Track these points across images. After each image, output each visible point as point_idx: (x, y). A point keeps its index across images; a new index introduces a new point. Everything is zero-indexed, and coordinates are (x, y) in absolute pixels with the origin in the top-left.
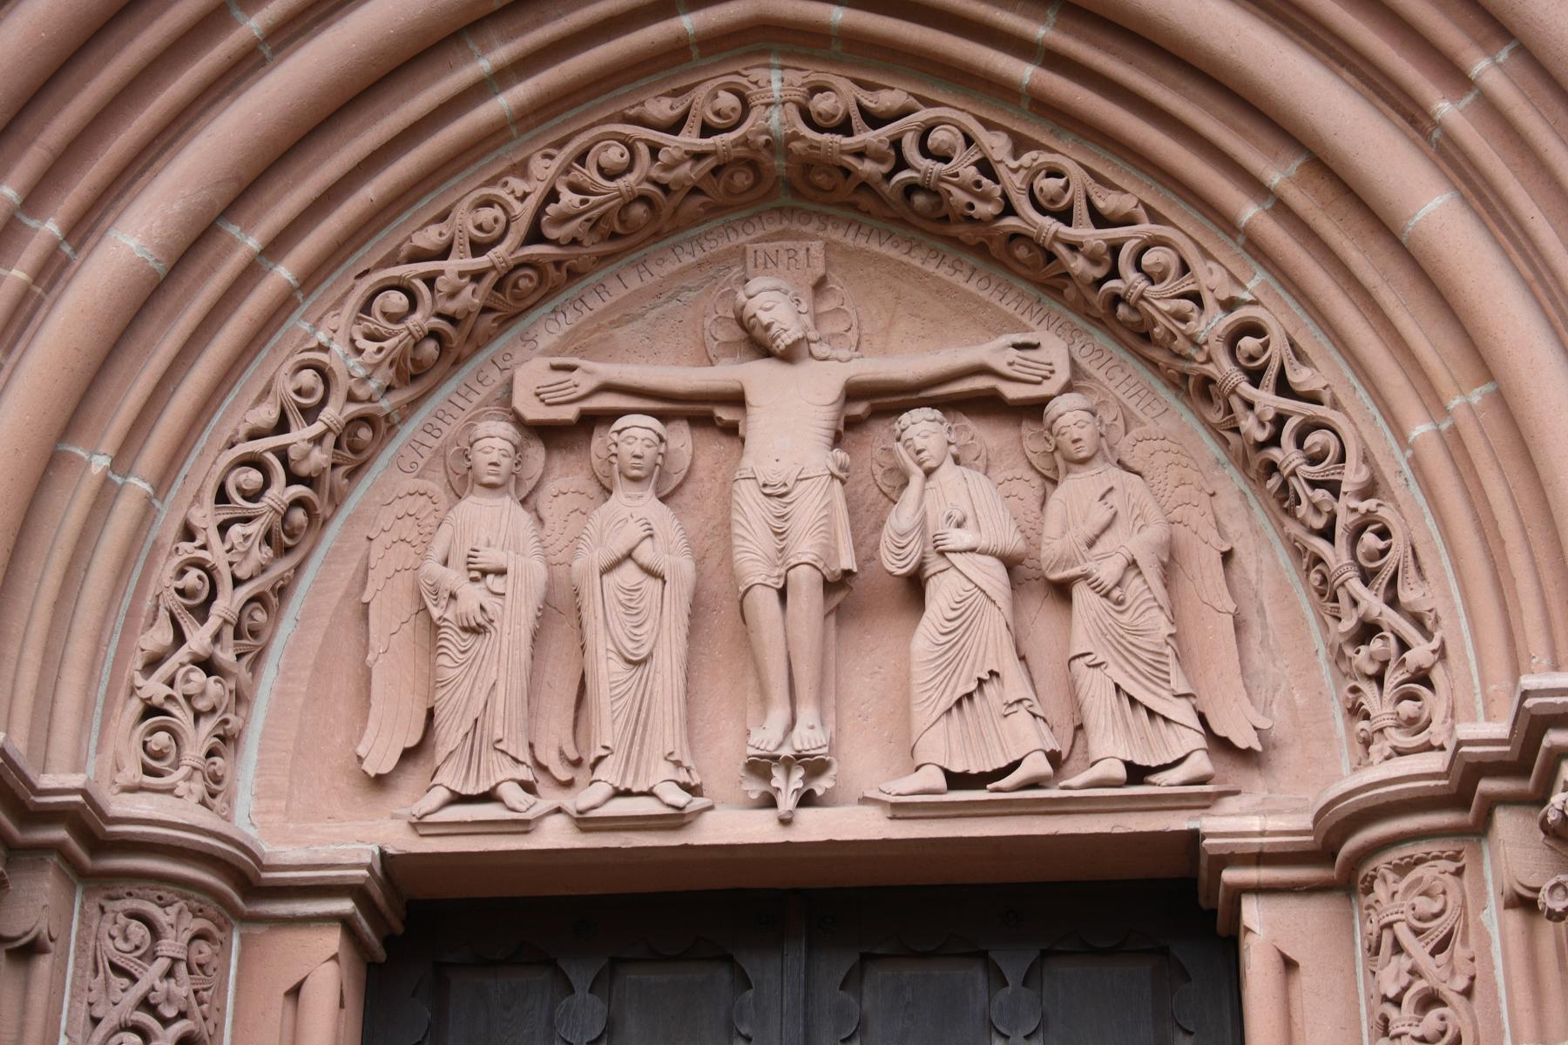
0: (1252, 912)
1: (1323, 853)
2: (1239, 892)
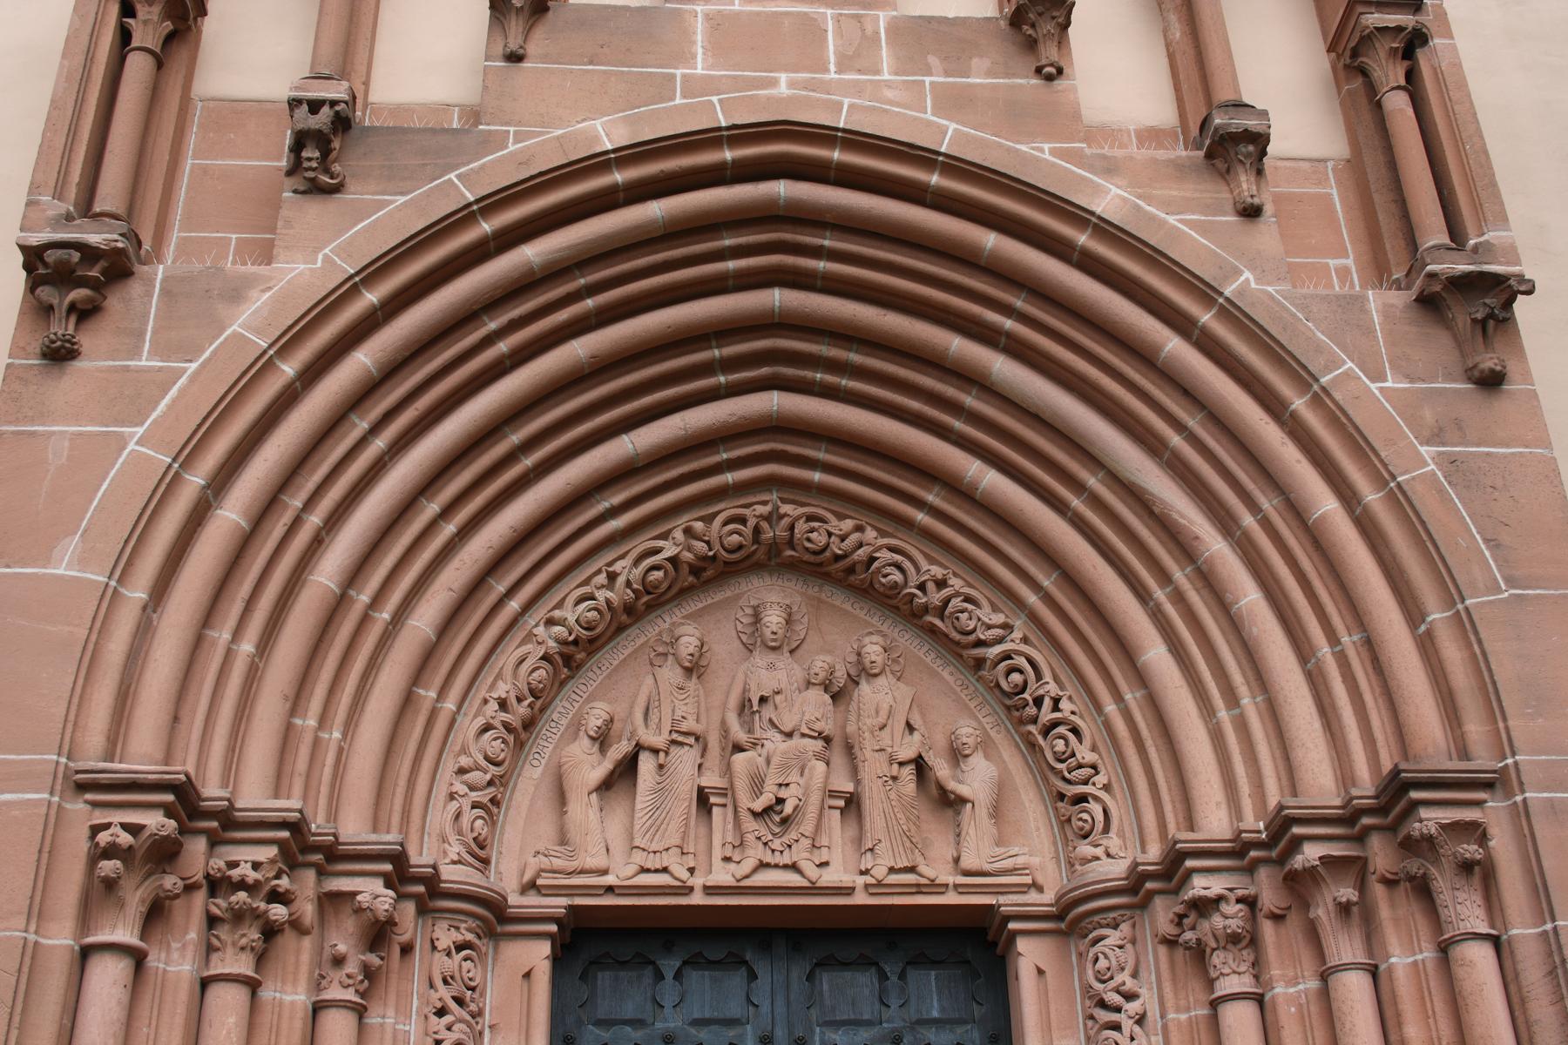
0: (1022, 944)
1: (1059, 917)
2: (1014, 934)
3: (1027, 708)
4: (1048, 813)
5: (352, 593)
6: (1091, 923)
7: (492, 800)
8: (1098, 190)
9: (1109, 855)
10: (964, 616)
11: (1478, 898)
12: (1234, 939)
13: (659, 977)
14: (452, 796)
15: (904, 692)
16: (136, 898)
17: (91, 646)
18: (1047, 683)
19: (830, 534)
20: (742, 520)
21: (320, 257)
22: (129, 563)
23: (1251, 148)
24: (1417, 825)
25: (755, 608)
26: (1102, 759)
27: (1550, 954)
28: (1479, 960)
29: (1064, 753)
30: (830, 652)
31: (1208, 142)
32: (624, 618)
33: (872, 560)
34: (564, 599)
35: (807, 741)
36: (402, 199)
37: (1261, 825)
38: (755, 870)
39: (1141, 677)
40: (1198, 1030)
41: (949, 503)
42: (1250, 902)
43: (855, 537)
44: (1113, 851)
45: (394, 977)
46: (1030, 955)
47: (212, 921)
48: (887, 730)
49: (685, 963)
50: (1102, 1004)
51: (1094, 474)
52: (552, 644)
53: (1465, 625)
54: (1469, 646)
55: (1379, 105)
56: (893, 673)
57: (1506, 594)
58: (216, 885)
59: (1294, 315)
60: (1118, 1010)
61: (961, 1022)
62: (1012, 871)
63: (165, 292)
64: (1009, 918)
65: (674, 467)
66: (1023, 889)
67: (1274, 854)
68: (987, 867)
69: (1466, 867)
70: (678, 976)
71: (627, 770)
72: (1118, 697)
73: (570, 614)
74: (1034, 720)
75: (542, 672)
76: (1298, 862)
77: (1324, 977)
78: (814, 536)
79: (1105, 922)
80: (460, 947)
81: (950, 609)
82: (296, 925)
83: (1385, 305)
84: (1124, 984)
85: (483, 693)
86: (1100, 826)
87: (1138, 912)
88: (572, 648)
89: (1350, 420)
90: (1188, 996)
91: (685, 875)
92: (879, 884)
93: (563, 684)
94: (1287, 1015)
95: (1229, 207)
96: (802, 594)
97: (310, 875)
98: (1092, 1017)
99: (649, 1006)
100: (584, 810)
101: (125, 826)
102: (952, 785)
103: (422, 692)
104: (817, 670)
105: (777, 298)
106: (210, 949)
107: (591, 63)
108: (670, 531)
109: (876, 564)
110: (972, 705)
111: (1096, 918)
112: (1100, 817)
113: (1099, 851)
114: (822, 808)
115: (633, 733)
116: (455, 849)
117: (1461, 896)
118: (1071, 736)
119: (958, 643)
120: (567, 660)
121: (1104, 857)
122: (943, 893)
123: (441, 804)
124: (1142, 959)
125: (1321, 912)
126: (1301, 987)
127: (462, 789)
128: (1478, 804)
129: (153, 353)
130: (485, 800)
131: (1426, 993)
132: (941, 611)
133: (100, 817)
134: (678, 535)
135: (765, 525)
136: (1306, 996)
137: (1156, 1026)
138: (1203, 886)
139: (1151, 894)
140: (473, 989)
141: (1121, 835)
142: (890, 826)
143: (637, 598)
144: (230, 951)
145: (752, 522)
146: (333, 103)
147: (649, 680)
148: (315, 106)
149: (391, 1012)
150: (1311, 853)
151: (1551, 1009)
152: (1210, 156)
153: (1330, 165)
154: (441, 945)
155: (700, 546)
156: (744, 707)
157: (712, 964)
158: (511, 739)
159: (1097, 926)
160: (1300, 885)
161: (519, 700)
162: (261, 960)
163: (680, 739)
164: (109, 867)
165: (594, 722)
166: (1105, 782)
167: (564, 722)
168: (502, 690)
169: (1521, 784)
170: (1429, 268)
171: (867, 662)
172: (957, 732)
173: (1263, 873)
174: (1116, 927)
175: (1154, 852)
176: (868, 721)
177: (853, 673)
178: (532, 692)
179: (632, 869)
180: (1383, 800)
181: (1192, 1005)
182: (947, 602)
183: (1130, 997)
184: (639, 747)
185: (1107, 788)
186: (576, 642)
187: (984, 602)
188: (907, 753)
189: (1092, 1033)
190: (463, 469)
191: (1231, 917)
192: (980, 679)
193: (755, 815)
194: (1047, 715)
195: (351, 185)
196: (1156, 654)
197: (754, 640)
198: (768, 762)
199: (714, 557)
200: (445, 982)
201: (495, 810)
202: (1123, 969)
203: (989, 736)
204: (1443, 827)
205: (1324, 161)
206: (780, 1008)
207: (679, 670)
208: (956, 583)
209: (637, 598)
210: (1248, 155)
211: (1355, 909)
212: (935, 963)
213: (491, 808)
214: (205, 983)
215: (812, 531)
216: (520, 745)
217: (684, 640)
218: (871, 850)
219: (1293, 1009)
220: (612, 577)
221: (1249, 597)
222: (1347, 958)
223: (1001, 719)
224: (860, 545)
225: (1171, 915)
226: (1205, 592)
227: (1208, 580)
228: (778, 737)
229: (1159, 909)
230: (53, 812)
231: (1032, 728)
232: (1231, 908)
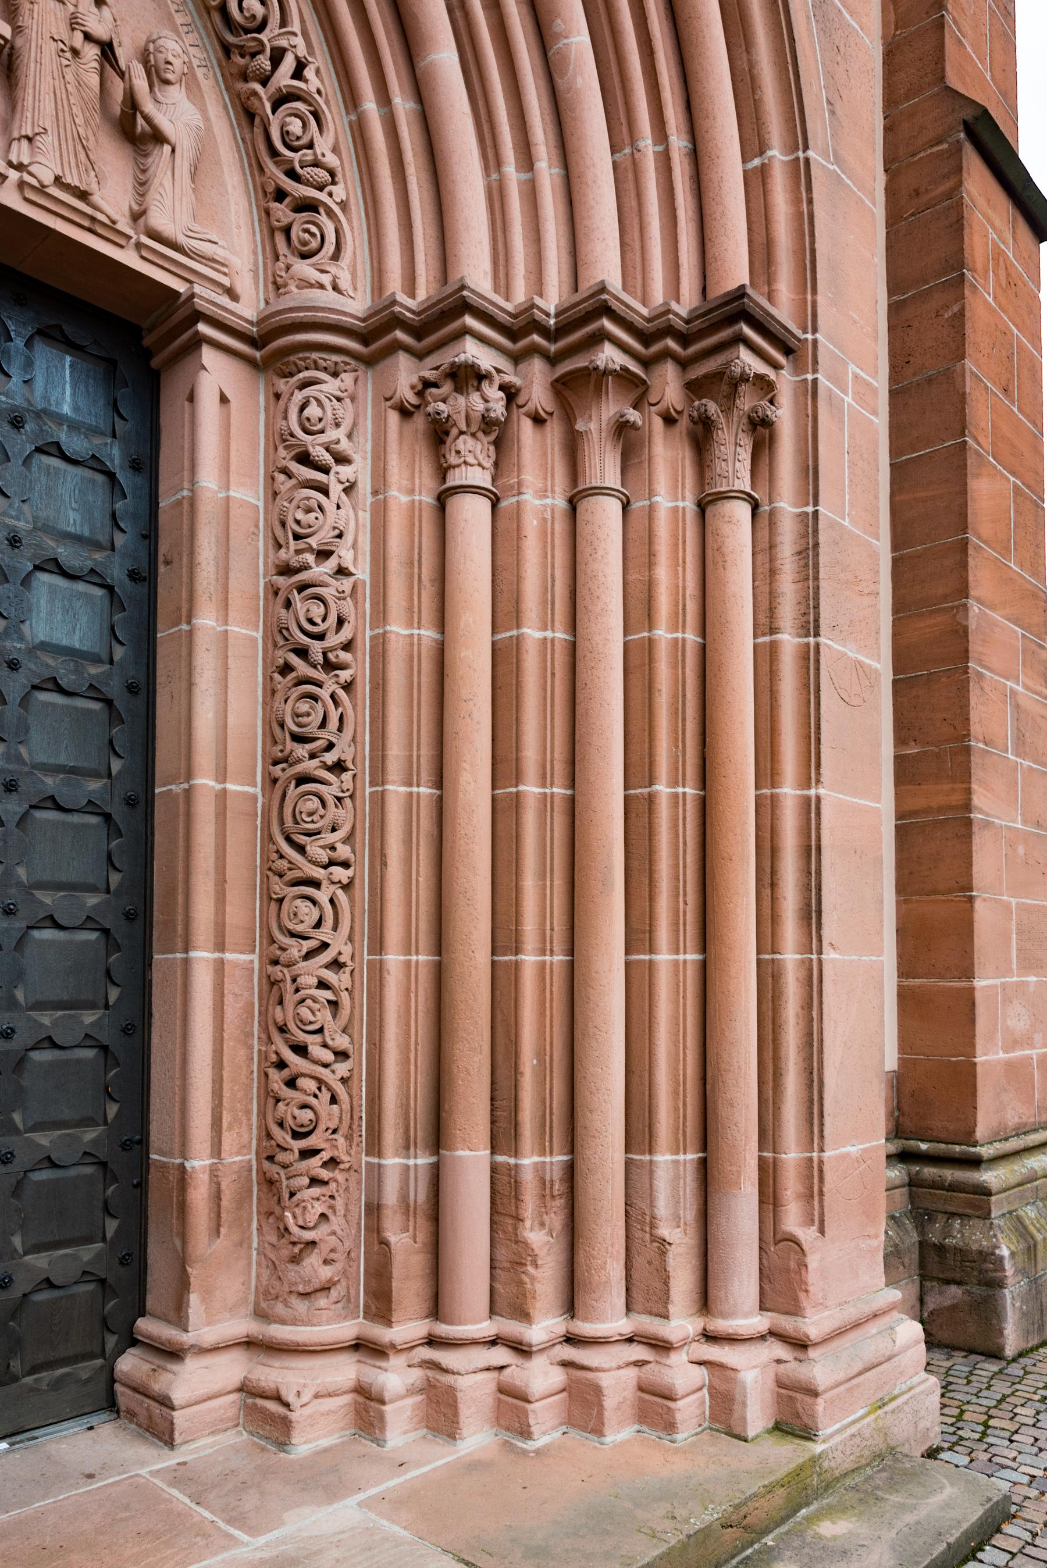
2: (200, 340)
3: (261, 56)
4: (251, 212)
6: (304, 359)
9: (335, 288)
18: (295, 34)
26: (343, 169)
29: (298, 138)
40: (420, 516)
60: (326, 470)
62: (209, 260)
64: (199, 316)
67: (553, 348)
68: (182, 240)
72: (384, 98)
79: (324, 364)
84: (338, 442)
86: (330, 248)
87: (362, 367)
90: (413, 477)
92: (41, 190)
111: (315, 355)
113: (326, 279)
121: (329, 288)
122: (122, 247)
124: (361, 421)
125: (593, 426)
126: (549, 501)
131: (680, 542)
136: (553, 511)
137: (365, 500)
142: (61, 118)
159: (313, 366)
166: (344, 199)
169: (815, 362)
172: (161, 42)
174: (335, 375)
181: (417, 489)
183: (342, 459)
189: (283, 489)
202: (338, 425)
203: (194, 75)
212: (71, 346)
218: (30, 139)
219: (535, 522)
223: (210, 61)
225: (415, 379)
229: (402, 368)
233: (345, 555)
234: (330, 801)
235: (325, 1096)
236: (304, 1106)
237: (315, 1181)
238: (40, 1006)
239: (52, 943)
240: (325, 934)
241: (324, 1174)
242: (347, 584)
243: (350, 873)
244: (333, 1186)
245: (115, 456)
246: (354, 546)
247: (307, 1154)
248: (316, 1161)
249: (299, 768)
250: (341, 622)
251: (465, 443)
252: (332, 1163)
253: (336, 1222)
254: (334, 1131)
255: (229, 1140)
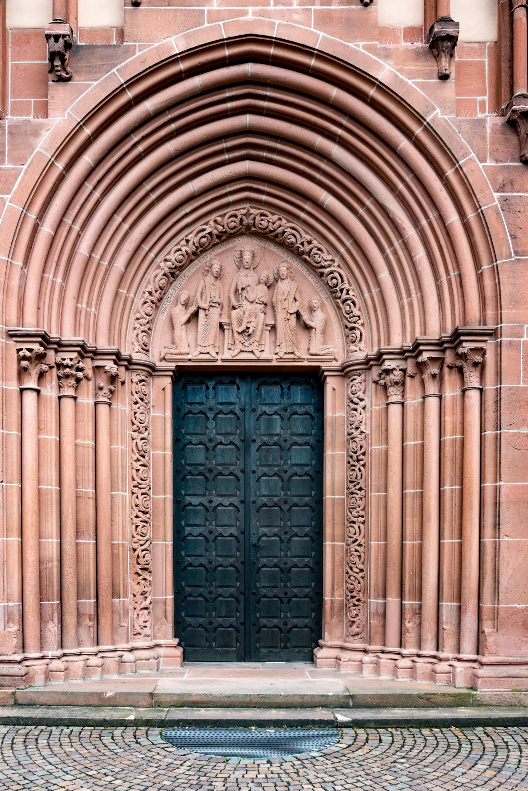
5: (93, 255)
7: (149, 329)
8: (381, 67)
10: (317, 256)
11: (478, 375)
12: (397, 383)
13: (208, 388)
14: (135, 328)
15: (294, 285)
16: (34, 372)
17: (6, 285)
19: (269, 222)
20: (236, 216)
21: (66, 113)
22: (14, 252)
23: (449, 44)
24: (461, 349)
25: (241, 251)
27: (497, 396)
28: (474, 396)
30: (268, 269)
31: (431, 39)
32: (193, 257)
33: (284, 232)
34: (170, 251)
35: (258, 305)
36: (95, 83)
37: (411, 344)
38: (239, 353)
39: (378, 284)
41: (314, 209)
42: (404, 371)
43: (278, 223)
44: (361, 349)
45: (120, 392)
46: (331, 383)
47: (59, 378)
48: (287, 301)
49: (216, 384)
50: (352, 401)
51: (369, 199)
52: (167, 269)
53: (495, 271)
54: (495, 280)
55: (512, 15)
56: (290, 277)
57: (513, 259)
58: (59, 366)
59: (454, 130)
60: (357, 404)
61: (307, 404)
63: (10, 133)
65: (209, 195)
66: (330, 360)
69: (476, 364)
70: (214, 388)
71: (196, 315)
73: (173, 257)
74: (340, 298)
75: (164, 280)
76: (420, 359)
77: (424, 398)
78: (262, 222)
80: (141, 381)
81: (312, 253)
82: (86, 377)
83: (494, 124)
85: (143, 290)
86: (358, 339)
88: (174, 270)
89: (468, 181)
91: (214, 355)
92: (281, 358)
93: (171, 283)
94: (410, 410)
95: (435, 75)
96: (259, 245)
97: (89, 361)
98: (349, 406)
99: (205, 398)
100: (180, 332)
101: (28, 350)
102: (309, 322)
103: (121, 291)
104: (262, 277)
105: (248, 120)
106: (60, 387)
107: (169, 5)
108: (208, 222)
109: (285, 234)
110: (318, 290)
111: (353, 372)
112: (359, 336)
113: (357, 348)
114: (262, 330)
115: (197, 302)
116: (137, 348)
117: (472, 374)
118: (352, 305)
119: (314, 266)
120: (173, 274)
123: (131, 332)
127: (138, 326)
128: (485, 341)
129: (10, 161)
130: (146, 329)
132: (309, 254)
133: (19, 346)
134: (212, 223)
135: (244, 218)
138: (388, 365)
139: (372, 366)
140: (146, 395)
141: (365, 343)
143: (197, 249)
144: (66, 388)
145: (239, 217)
146: (64, 36)
147: (202, 282)
148: (57, 38)
149: (119, 404)
150: (425, 356)
151: (494, 414)
152: (431, 47)
153: (487, 44)
154: (134, 381)
155: (220, 228)
156: (236, 291)
157: (225, 384)
158: (154, 306)
160: (421, 367)
161: (156, 291)
162: (76, 389)
163: (213, 305)
164: (24, 363)
165: (183, 299)
167: (173, 298)
168: (150, 288)
170: (514, 107)
171: (281, 274)
173: (409, 361)
174: (360, 376)
175: (375, 350)
176: (280, 297)
177: (276, 277)
178: (160, 288)
179: (198, 353)
180: (452, 338)
182: (311, 250)
183: (361, 400)
184: (199, 308)
185: (362, 325)
186: (175, 268)
187: (325, 250)
188: (293, 310)
190: (129, 201)
191: (396, 376)
192: (322, 280)
193: (239, 333)
194: (344, 296)
195: (75, 77)
196: (384, 275)
197: (240, 265)
198: (244, 313)
199: (225, 232)
200: (137, 393)
201: (149, 332)
204: (471, 350)
205: (485, 43)
206: (248, 400)
207: (213, 278)
208: (315, 242)
209: (197, 249)
210: (447, 48)
211: (438, 376)
213: (148, 332)
214: (60, 398)
215: (262, 220)
216: (157, 307)
217: (214, 266)
220: (187, 241)
221: (420, 254)
222: (432, 392)
224: (280, 226)
226: (405, 251)
227: (406, 246)
228: (248, 303)
230: (4, 345)
231: (338, 301)
232: (397, 373)
233: (362, 428)
234: (358, 499)
235: (357, 582)
236: (352, 584)
237: (355, 605)
238: (294, 557)
239: (297, 541)
240: (356, 537)
241: (357, 603)
242: (363, 436)
243: (364, 519)
244: (360, 607)
245: (311, 409)
246: (365, 424)
247: (353, 597)
248: (354, 599)
249: (351, 490)
250: (361, 447)
251: (390, 390)
252: (359, 600)
253: (360, 616)
254: (359, 591)
255: (336, 593)
